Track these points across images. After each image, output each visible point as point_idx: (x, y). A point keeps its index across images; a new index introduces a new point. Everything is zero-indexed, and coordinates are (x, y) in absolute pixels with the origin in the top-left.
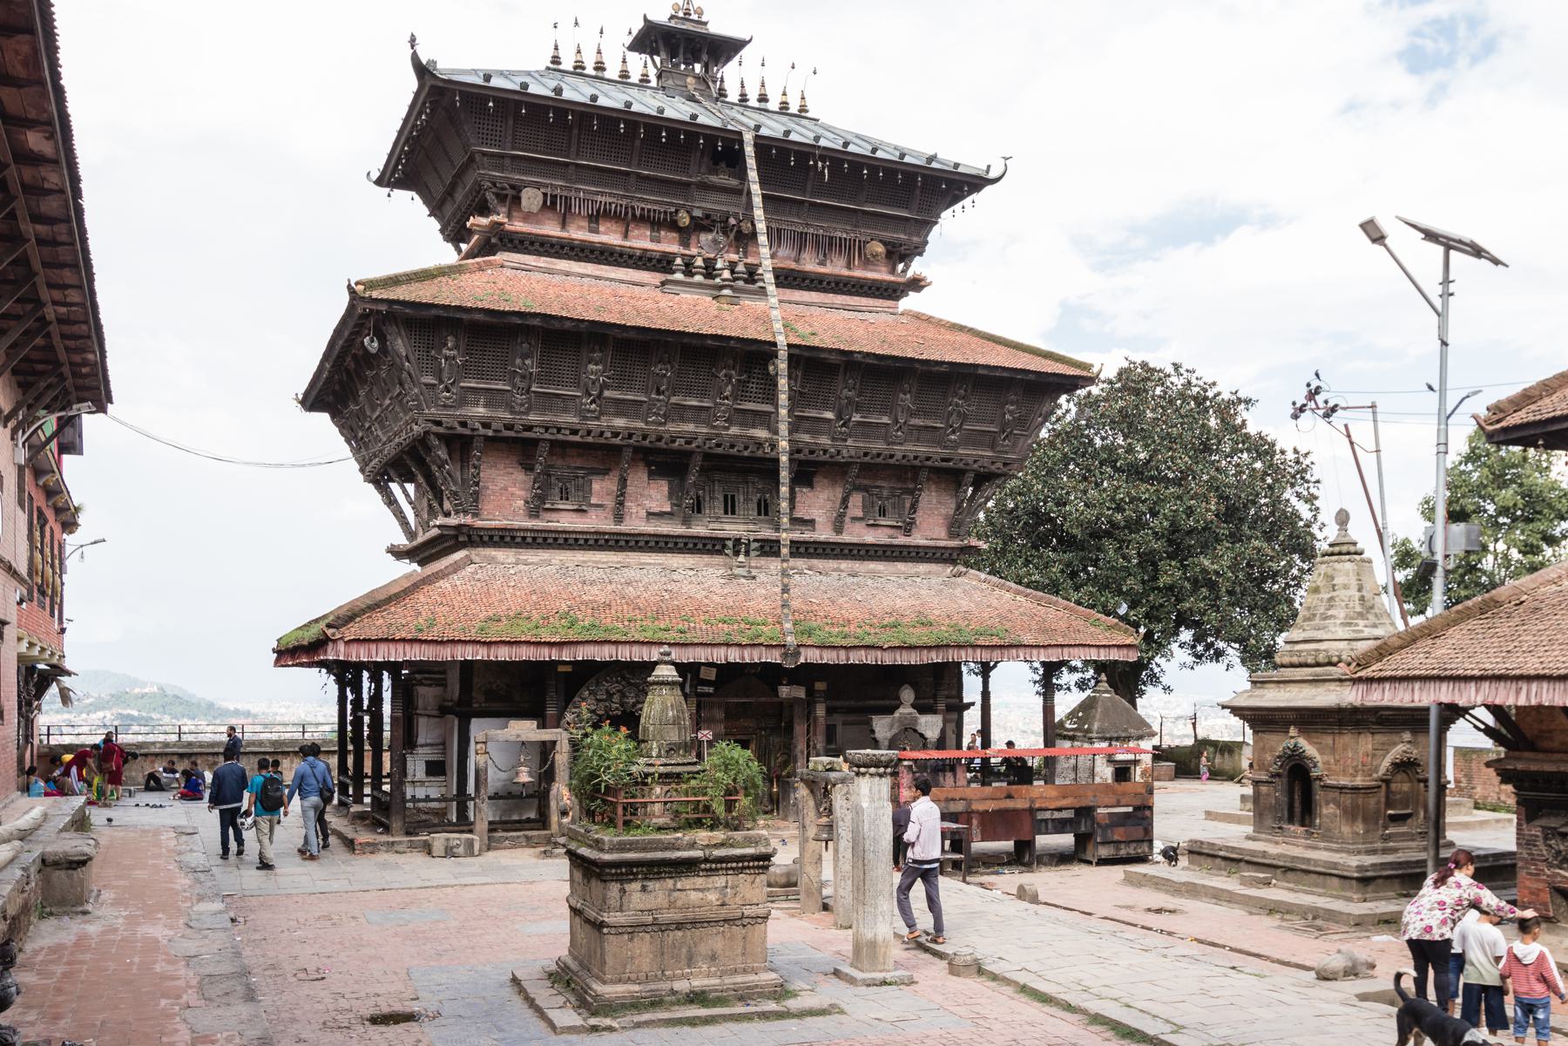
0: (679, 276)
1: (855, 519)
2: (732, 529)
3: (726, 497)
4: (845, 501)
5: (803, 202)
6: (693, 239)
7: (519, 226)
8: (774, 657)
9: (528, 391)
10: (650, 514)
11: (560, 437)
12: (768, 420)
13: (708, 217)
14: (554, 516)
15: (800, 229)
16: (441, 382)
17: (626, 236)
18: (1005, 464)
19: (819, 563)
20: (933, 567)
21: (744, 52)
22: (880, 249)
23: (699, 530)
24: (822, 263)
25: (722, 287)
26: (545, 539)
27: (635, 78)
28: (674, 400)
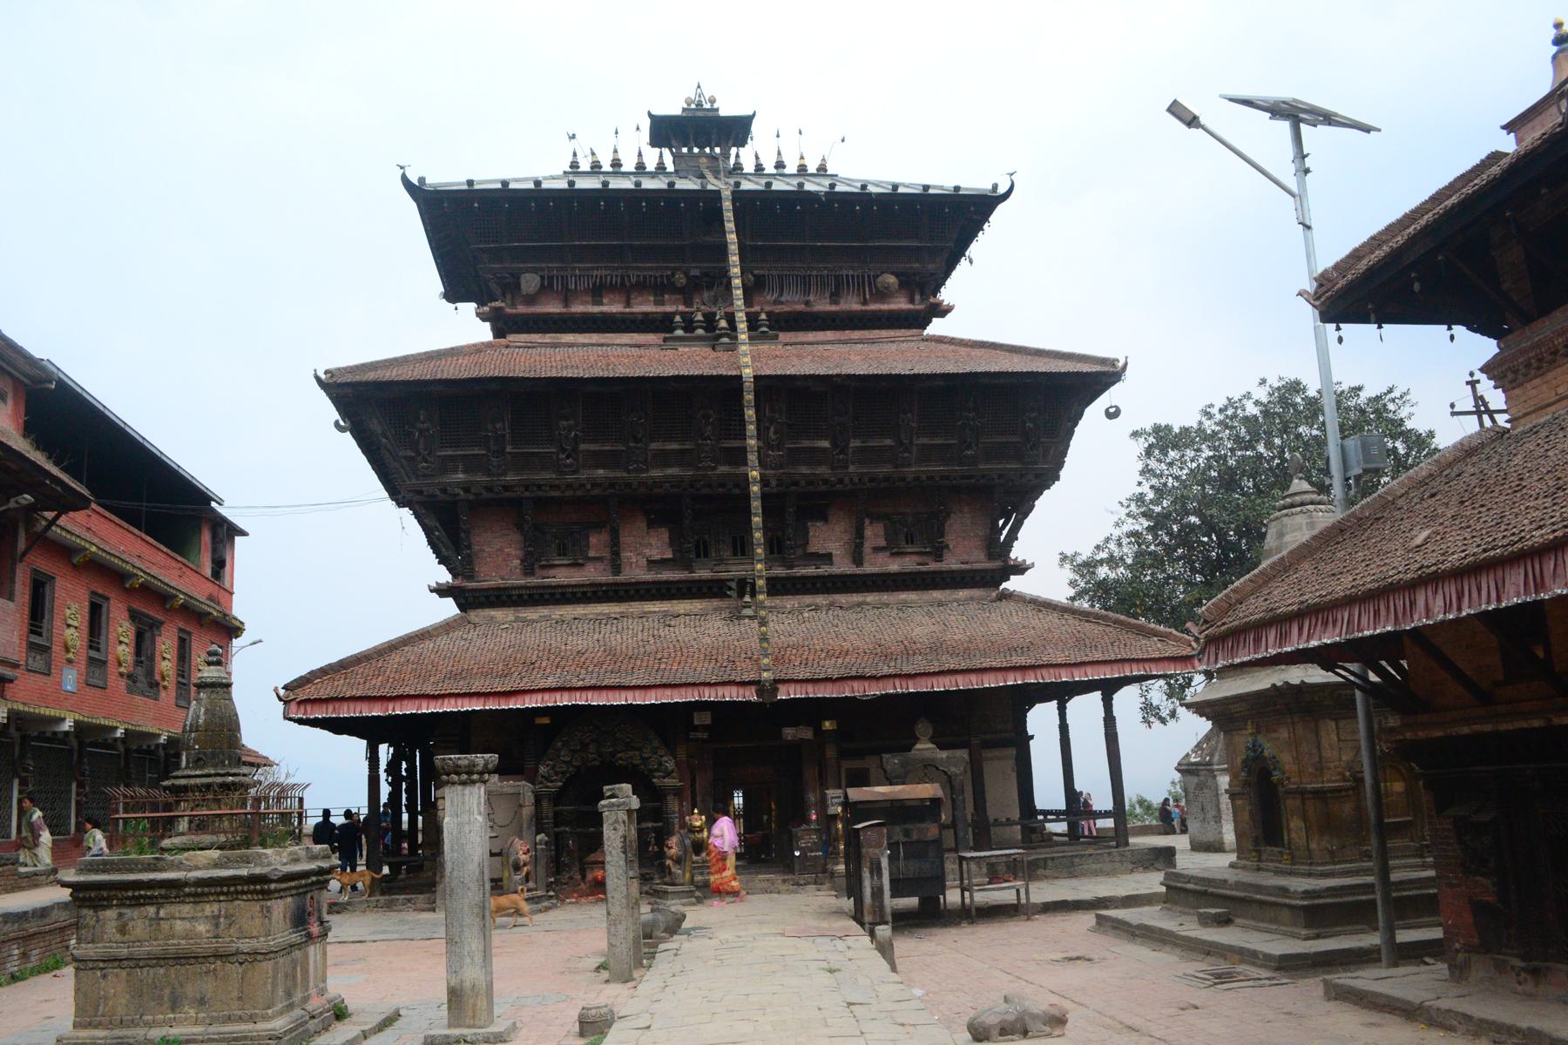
0: (679, 332)
1: (877, 549)
2: (735, 571)
3: (734, 539)
4: (859, 534)
5: (803, 247)
6: (697, 300)
7: (522, 309)
8: (751, 695)
9: (503, 451)
10: (652, 564)
11: (540, 493)
12: (739, 456)
13: (706, 274)
14: (552, 572)
15: (803, 273)
16: (418, 453)
17: (628, 304)
18: (1037, 476)
19: (842, 599)
20: (976, 593)
21: (753, 128)
22: (891, 280)
23: (703, 574)
24: (837, 303)
25: (721, 336)
26: (542, 595)
27: (651, 166)
28: (654, 446)
